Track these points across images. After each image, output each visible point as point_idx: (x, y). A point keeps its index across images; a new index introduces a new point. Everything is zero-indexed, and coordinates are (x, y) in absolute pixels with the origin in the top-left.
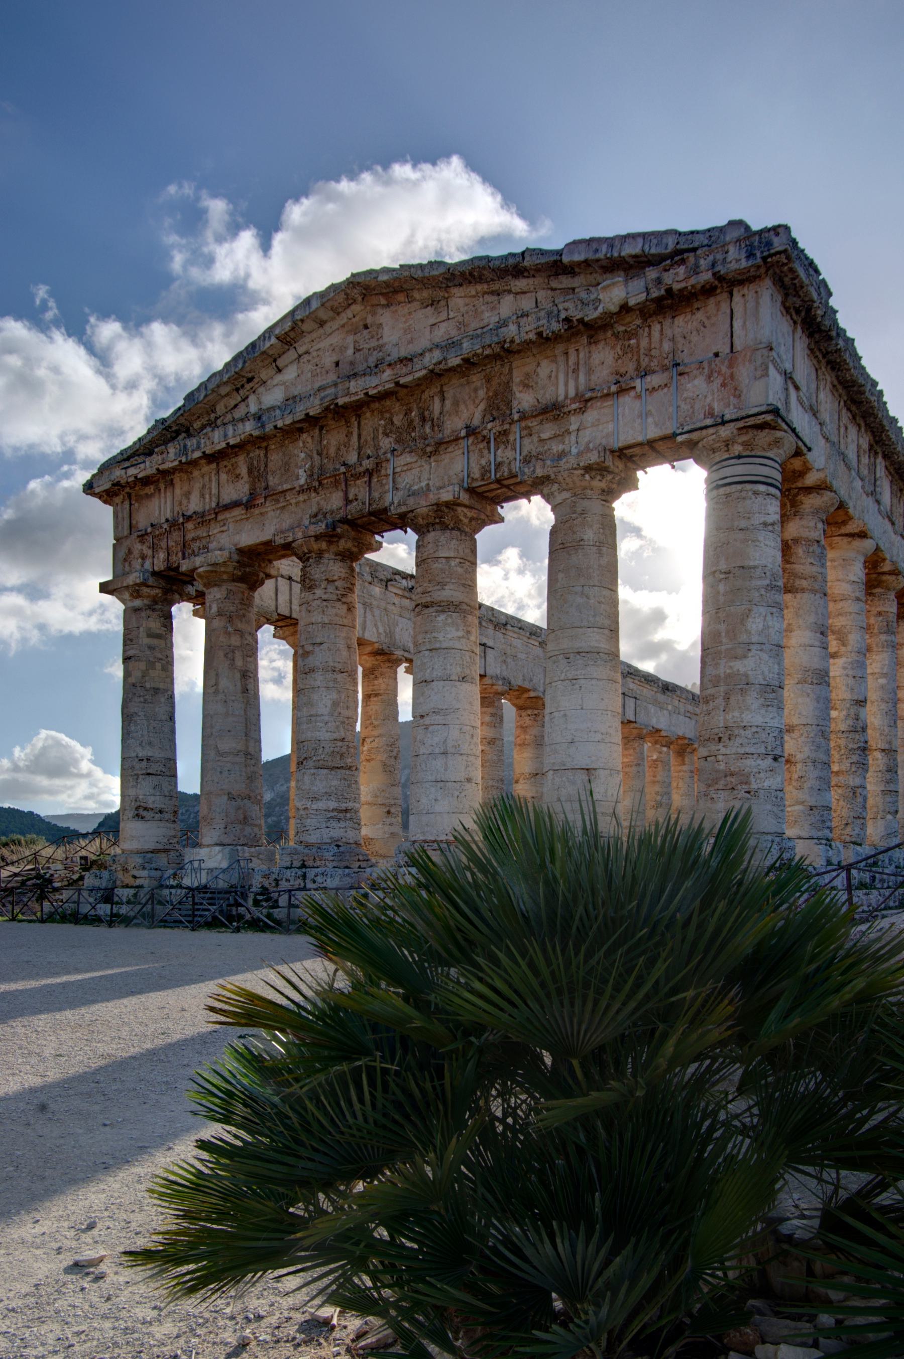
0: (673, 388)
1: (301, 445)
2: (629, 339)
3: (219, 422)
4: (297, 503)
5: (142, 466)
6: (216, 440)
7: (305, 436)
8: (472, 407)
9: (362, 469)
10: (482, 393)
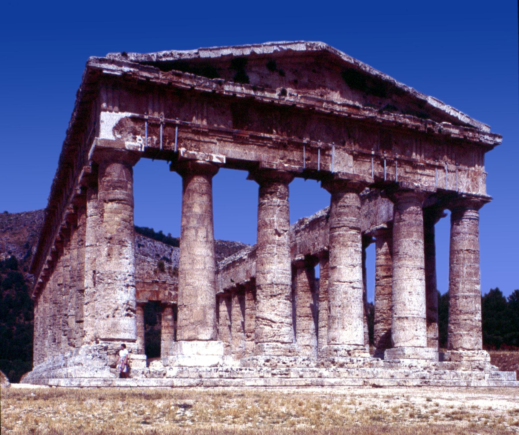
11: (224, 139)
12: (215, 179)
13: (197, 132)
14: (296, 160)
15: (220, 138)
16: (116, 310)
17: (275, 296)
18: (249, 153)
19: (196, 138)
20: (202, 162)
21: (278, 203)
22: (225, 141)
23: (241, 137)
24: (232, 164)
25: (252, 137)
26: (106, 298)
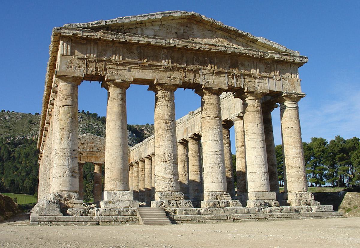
0: (281, 81)
1: (163, 52)
2: (268, 65)
3: (122, 31)
4: (161, 71)
5: (93, 34)
6: (134, 39)
7: (165, 50)
8: (225, 64)
9: (190, 69)
10: (229, 62)
11: (132, 67)
12: (127, 91)
13: (117, 64)
14: (178, 78)
15: (130, 67)
16: (66, 172)
17: (166, 161)
18: (148, 75)
19: (116, 67)
20: (118, 81)
21: (166, 104)
22: (134, 68)
23: (143, 66)
24: (137, 81)
25: (150, 65)
26: (59, 165)
